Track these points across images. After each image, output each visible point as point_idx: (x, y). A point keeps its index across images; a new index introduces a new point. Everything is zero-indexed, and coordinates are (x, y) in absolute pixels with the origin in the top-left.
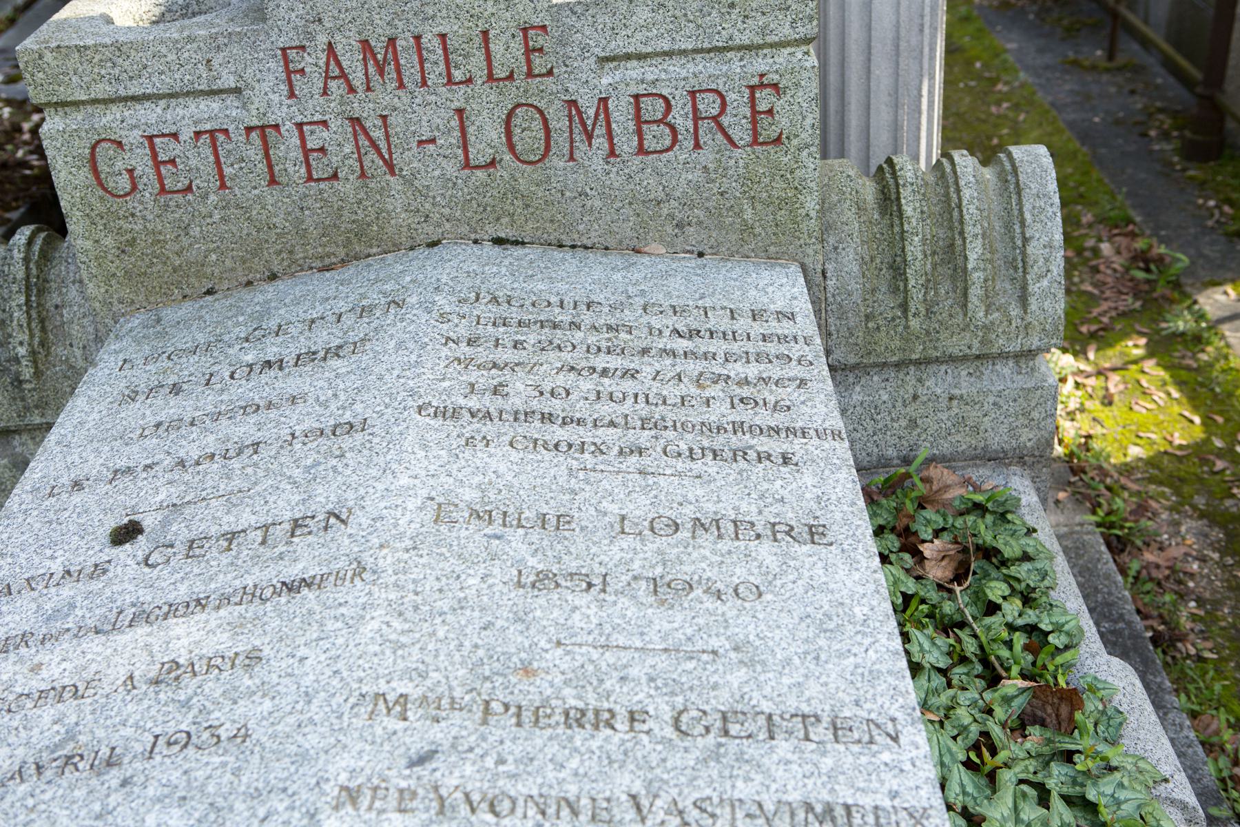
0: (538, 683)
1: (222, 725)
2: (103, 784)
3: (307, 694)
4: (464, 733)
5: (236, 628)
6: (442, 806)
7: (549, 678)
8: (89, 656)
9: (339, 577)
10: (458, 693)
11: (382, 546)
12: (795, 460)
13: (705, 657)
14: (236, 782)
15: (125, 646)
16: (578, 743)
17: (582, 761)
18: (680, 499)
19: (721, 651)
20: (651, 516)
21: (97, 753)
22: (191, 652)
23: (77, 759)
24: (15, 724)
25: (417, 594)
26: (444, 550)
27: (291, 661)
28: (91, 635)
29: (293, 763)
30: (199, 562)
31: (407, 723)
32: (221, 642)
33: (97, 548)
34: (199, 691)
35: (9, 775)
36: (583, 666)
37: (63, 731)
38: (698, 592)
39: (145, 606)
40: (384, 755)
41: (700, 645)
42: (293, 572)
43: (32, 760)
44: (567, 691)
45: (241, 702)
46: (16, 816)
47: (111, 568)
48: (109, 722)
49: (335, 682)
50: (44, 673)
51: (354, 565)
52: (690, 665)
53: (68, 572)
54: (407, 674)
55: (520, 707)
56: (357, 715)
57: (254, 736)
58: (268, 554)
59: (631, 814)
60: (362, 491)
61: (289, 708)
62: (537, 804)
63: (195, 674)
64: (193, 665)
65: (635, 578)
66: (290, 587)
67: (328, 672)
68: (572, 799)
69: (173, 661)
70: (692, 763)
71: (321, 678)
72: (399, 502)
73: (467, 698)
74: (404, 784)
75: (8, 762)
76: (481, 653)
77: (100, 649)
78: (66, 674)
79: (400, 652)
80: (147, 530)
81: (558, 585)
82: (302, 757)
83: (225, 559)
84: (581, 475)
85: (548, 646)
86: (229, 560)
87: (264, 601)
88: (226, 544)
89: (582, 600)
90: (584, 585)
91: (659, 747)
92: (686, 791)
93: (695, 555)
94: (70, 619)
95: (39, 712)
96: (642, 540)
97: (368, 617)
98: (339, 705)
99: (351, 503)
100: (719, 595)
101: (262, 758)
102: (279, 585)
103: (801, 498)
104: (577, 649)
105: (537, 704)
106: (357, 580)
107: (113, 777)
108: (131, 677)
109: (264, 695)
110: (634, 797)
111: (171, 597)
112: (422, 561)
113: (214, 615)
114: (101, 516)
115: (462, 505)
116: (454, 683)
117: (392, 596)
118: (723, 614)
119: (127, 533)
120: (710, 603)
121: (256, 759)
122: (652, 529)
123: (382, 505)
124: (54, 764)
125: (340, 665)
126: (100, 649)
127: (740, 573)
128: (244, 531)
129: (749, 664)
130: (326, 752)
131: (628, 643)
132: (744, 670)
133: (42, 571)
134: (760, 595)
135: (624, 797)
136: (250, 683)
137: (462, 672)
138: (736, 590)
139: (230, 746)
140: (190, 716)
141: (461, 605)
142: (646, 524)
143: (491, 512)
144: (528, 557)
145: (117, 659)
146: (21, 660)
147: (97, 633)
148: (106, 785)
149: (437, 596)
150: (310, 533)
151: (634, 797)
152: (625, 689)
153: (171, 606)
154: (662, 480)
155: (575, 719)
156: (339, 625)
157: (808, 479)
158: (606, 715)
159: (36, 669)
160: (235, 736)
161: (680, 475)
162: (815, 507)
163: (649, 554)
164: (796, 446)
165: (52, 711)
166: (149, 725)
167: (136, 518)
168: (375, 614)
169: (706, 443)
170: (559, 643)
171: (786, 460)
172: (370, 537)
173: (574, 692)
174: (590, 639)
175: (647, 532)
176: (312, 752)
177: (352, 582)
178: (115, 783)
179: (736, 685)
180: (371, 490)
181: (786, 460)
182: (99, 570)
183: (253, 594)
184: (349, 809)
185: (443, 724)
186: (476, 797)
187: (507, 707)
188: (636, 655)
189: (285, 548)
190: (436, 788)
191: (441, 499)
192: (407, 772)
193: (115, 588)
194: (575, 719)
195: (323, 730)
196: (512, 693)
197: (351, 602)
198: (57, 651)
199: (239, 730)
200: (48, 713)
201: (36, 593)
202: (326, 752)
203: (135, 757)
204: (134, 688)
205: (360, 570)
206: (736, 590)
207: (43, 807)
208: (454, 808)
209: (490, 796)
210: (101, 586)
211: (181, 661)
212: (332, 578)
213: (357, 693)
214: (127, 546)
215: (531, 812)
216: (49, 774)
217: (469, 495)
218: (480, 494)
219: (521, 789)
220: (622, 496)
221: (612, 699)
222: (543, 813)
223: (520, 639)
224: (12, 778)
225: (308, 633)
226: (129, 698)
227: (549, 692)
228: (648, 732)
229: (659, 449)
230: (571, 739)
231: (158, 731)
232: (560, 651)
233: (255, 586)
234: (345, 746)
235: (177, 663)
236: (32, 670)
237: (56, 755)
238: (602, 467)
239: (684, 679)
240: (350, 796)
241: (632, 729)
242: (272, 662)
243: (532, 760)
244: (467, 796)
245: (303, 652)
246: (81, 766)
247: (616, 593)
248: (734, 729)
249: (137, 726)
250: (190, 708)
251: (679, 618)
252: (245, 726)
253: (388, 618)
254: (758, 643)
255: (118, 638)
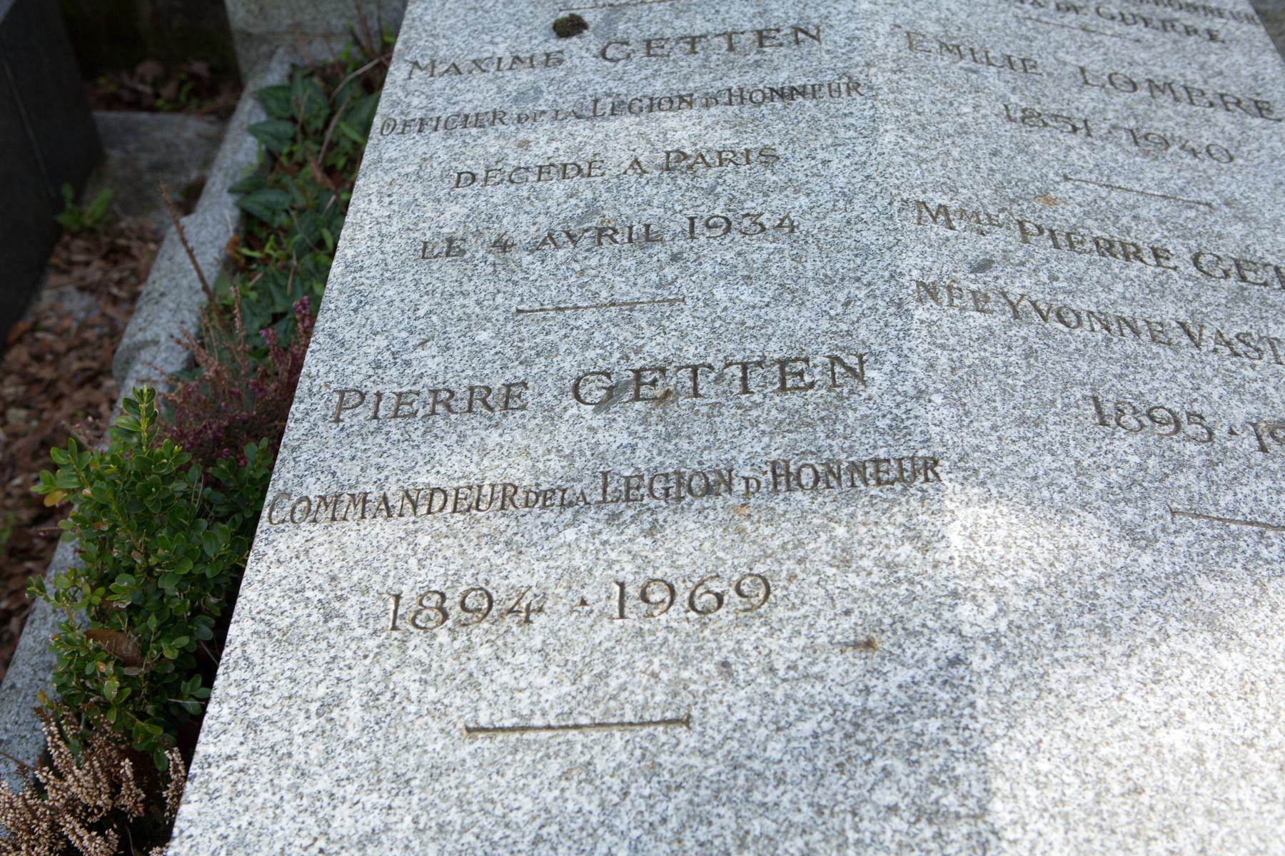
0: (1061, 211)
1: (761, 214)
2: (650, 256)
3: (844, 194)
4: (1010, 248)
5: (737, 126)
6: (1015, 311)
7: (1069, 208)
8: (579, 139)
9: (833, 91)
10: (991, 210)
11: (868, 65)
12: (1221, 36)
13: (1201, 207)
14: (800, 268)
15: (616, 133)
16: (1117, 271)
17: (1126, 287)
18: (1128, 59)
19: (1214, 204)
20: (1108, 71)
21: (631, 228)
22: (695, 144)
23: (610, 232)
24: (526, 194)
25: (919, 114)
26: (928, 76)
27: (813, 162)
28: (573, 120)
29: (856, 256)
30: (666, 62)
31: (950, 233)
32: (721, 137)
33: (541, 38)
34: (721, 181)
35: (540, 240)
36: (1095, 201)
37: (582, 204)
38: (1174, 148)
39: (622, 97)
40: (945, 259)
41: (1193, 197)
42: (781, 79)
43: (559, 228)
44: (1089, 222)
45: (773, 196)
46: (566, 278)
47: (566, 57)
48: (630, 201)
49: (871, 186)
50: (535, 150)
51: (845, 80)
52: (1192, 214)
53: (517, 58)
54: (937, 186)
55: (1052, 232)
56: (906, 219)
57: (801, 228)
58: (742, 61)
59: (1185, 340)
60: (823, 11)
61: (829, 206)
62: (1099, 320)
63: (708, 166)
64: (703, 158)
65: (1114, 127)
66: (786, 94)
67: (860, 178)
68: (1129, 319)
69: (678, 151)
70: (1223, 301)
71: (854, 181)
72: (869, 25)
73: (1001, 216)
74: (974, 287)
75: (533, 229)
76: (998, 176)
77: (587, 132)
78: (561, 152)
79: (924, 166)
80: (592, 26)
81: (1046, 125)
82: (864, 252)
83: (695, 61)
84: (1029, 23)
85: (1058, 179)
86: (699, 62)
87: (759, 104)
88: (688, 47)
89: (1074, 141)
90: (1070, 128)
91: (1190, 284)
92: (1227, 325)
93: (1160, 113)
94: (541, 101)
95: (547, 185)
96: (1108, 92)
97: (882, 130)
98: (886, 208)
99: (816, 21)
100: (1194, 153)
101: (820, 249)
102: (767, 91)
103: (1237, 73)
104: (1084, 185)
105: (1067, 230)
106: (854, 94)
107: (660, 252)
108: (636, 161)
109: (796, 192)
110: (1182, 325)
111: (649, 91)
112: (913, 83)
113: (705, 113)
114: (531, 8)
115: (929, 37)
116: (985, 201)
117: (897, 113)
118: (1205, 171)
119: (570, 27)
120: (1188, 160)
121: (813, 248)
122: (1112, 83)
123: (852, 25)
124: (586, 234)
125: (869, 171)
126: (587, 132)
127: (1206, 137)
128: (705, 36)
129: (1244, 219)
130: (890, 249)
131: (1129, 186)
132: (1240, 224)
133: (487, 55)
134: (1231, 159)
135: (1174, 324)
136: (774, 178)
137: (987, 192)
138: (1208, 151)
139: (778, 234)
140: (721, 202)
141: (963, 130)
142: (1105, 78)
143: (958, 47)
144: (1009, 95)
145: (611, 144)
146: (501, 136)
147: (578, 117)
148: (655, 259)
149: (938, 119)
150: (781, 45)
151: (1182, 325)
152: (1141, 227)
153: (651, 99)
154: (1105, 39)
155: (1107, 248)
156: (852, 133)
157: (1238, 57)
158: (1132, 249)
159: (525, 145)
160: (780, 226)
161: (1120, 36)
162: (1253, 84)
163: (1118, 107)
164: (1217, 24)
165: (562, 186)
166: (678, 208)
167: (578, 13)
168: (888, 127)
169: (1134, 10)
170: (1066, 178)
171: (1213, 37)
172: (851, 55)
173: (1096, 224)
174: (1093, 177)
175: (1108, 86)
176: (873, 247)
177: (849, 94)
178: (663, 257)
179: (1238, 237)
180: (835, 12)
181: (1213, 37)
182: (550, 60)
183: (741, 97)
184: (933, 303)
185: (988, 236)
186: (1043, 307)
187: (1041, 232)
188: (1140, 198)
189: (758, 57)
190: (1004, 295)
191: (908, 28)
192: (972, 276)
193: (580, 78)
194: (1107, 248)
195: (876, 228)
196: (1040, 217)
197: (857, 113)
198: (540, 130)
199: (783, 220)
200: (558, 189)
201: (490, 76)
202: (890, 249)
203: (675, 235)
204: (645, 172)
205: (854, 86)
206: (1208, 151)
207: (593, 272)
208: (1027, 314)
209: (1055, 307)
210: (562, 74)
211: (688, 151)
212: (825, 89)
213: (898, 198)
214: (575, 39)
215: (1097, 327)
216: (585, 243)
217: (933, 28)
218: (941, 29)
219: (1082, 304)
220: (1073, 49)
221: (1132, 234)
222: (1108, 329)
223: (1029, 169)
224: (544, 243)
225: (821, 138)
226: (643, 181)
227: (1073, 221)
228: (1175, 268)
229: (1093, 9)
230: (1109, 266)
231: (691, 213)
232: (1069, 185)
233: (741, 90)
234: (907, 247)
235: (683, 154)
236: (520, 146)
237: (586, 226)
238: (1045, 19)
239: (1190, 226)
240: (928, 291)
241: (1159, 265)
242: (791, 161)
243: (1080, 279)
244: (1034, 304)
245: (821, 155)
246: (618, 238)
247: (1101, 138)
248: (1250, 276)
249: (663, 205)
250: (718, 196)
251: (1166, 169)
252: (787, 217)
253: (900, 133)
254: (1245, 202)
255: (605, 124)
